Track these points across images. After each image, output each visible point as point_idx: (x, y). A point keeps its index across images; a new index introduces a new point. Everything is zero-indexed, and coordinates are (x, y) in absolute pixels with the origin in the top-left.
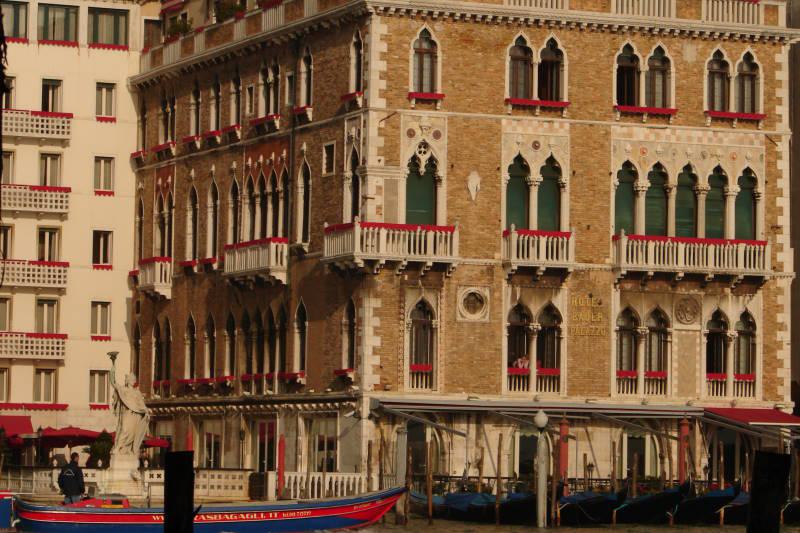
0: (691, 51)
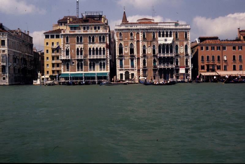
0: (97, 36)
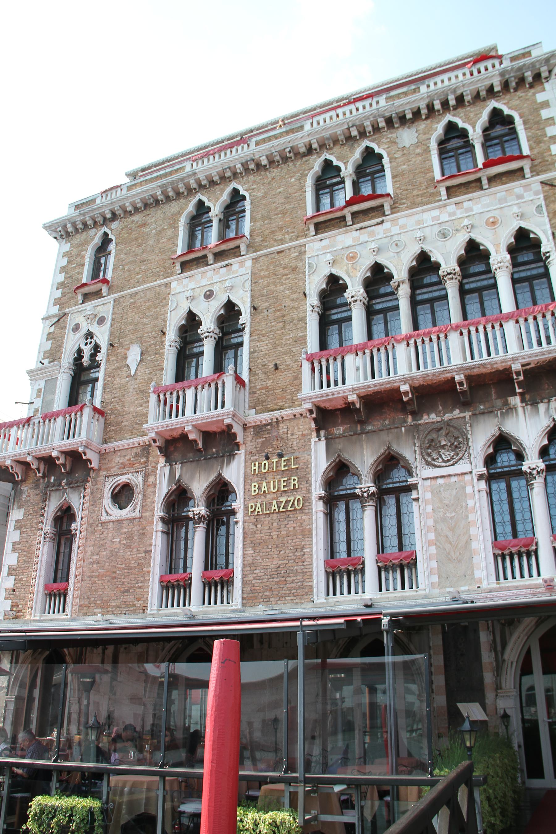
0: (407, 137)
